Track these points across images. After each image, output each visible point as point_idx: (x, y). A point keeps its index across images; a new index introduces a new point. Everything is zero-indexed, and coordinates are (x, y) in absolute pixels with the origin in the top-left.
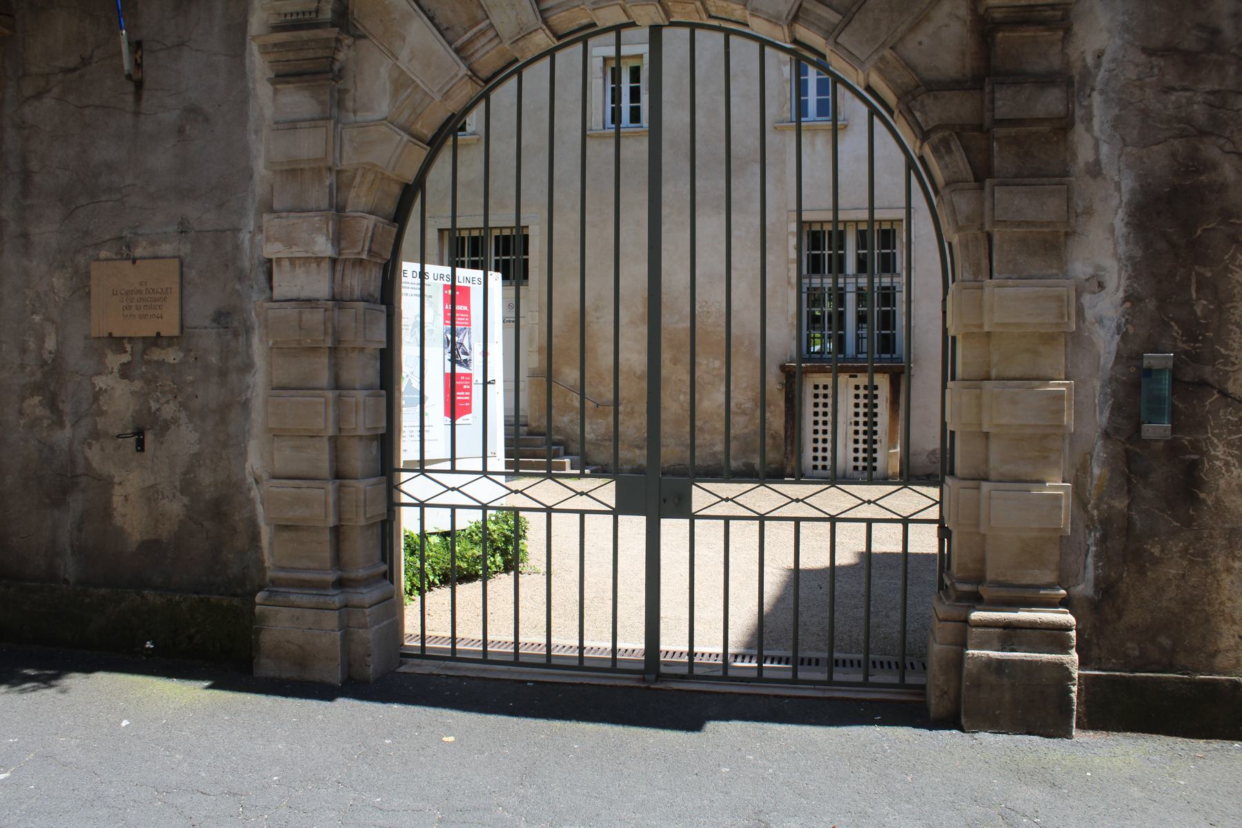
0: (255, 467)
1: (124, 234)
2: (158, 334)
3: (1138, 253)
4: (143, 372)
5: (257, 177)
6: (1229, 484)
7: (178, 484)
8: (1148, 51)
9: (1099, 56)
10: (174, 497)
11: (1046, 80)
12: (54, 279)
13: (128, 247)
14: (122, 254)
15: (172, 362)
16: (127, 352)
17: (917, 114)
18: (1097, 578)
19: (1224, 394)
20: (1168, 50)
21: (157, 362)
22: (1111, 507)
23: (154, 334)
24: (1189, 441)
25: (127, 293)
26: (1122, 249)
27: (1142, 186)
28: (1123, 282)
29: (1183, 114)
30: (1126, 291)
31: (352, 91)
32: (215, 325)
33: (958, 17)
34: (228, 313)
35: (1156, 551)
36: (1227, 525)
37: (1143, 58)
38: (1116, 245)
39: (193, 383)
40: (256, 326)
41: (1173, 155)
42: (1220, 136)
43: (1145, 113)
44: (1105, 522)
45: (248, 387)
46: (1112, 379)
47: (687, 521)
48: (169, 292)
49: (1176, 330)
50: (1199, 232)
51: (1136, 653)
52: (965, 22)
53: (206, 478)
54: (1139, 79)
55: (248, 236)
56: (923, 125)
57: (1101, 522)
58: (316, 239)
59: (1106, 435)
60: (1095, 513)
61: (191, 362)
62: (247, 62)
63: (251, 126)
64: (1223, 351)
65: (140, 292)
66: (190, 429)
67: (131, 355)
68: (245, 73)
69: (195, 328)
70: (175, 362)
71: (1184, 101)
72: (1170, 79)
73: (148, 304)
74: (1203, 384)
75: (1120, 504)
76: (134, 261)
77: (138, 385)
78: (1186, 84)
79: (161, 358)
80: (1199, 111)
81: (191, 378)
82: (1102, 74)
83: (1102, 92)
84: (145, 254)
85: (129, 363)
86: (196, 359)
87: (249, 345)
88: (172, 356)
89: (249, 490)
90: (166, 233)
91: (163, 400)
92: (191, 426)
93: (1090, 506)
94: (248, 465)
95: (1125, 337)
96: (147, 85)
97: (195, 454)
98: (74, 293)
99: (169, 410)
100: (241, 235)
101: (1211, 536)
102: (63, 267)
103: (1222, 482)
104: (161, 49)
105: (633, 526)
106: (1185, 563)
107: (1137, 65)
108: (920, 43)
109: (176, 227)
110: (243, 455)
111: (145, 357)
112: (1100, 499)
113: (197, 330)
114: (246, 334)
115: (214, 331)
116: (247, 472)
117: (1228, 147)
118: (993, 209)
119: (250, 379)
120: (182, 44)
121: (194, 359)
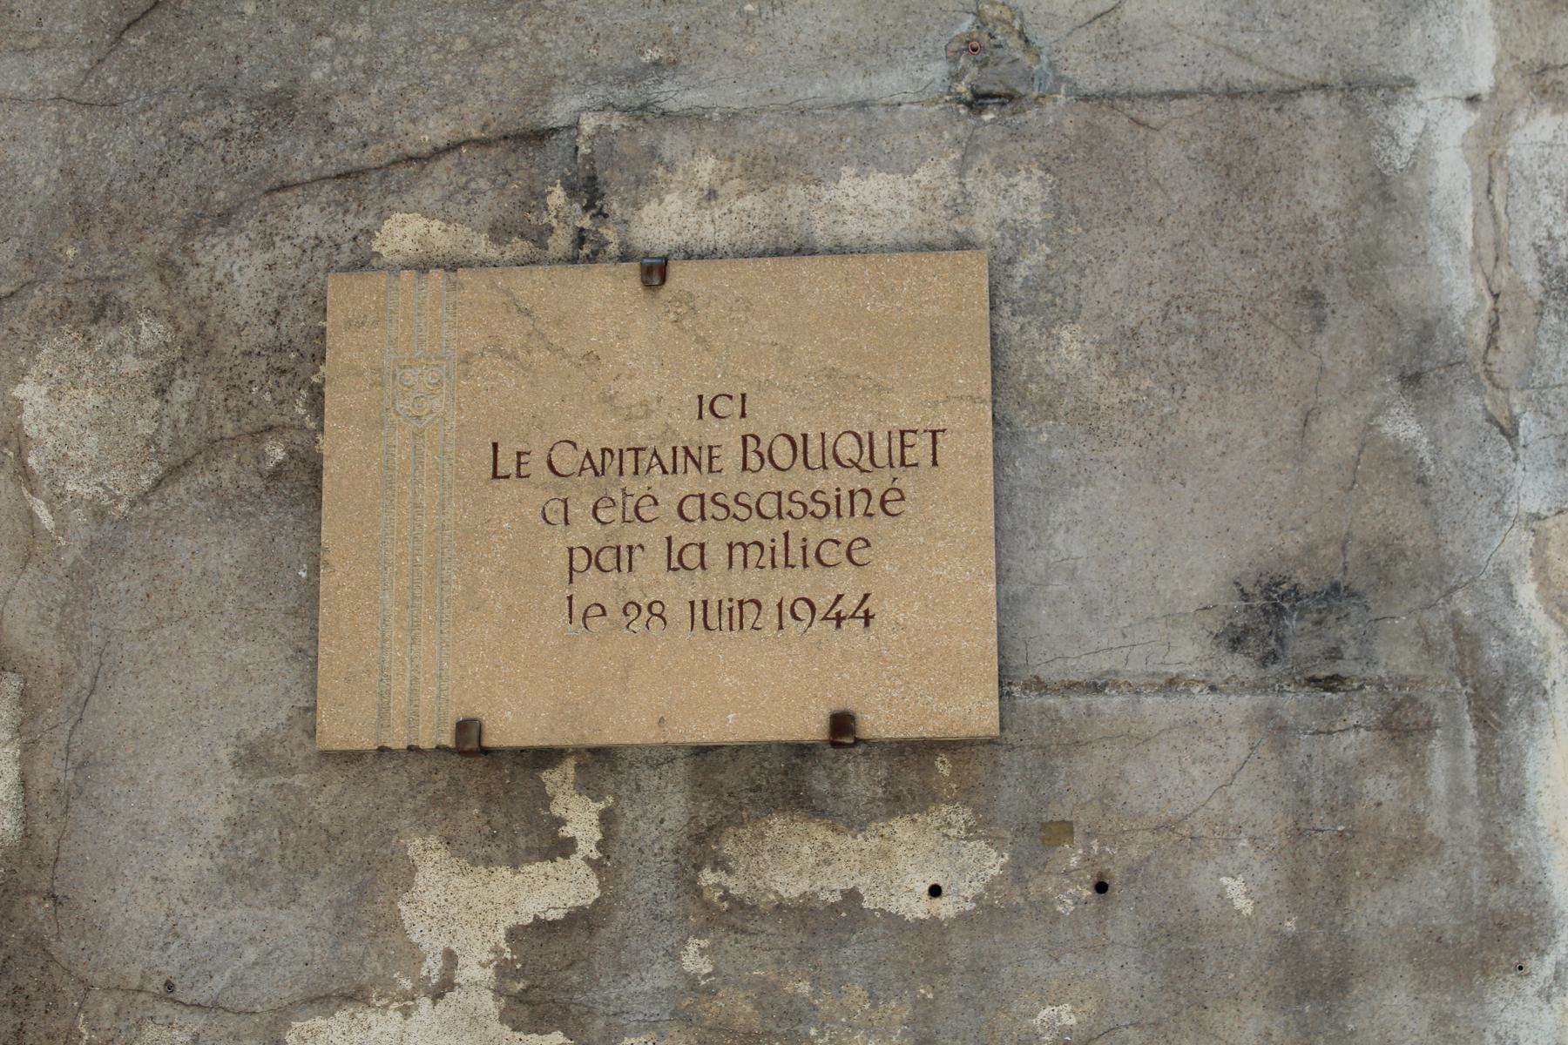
1: (559, 114)
2: (842, 724)
4: (692, 980)
12: (30, 392)
13: (589, 191)
14: (540, 236)
15: (917, 907)
16: (565, 848)
21: (803, 913)
23: (814, 728)
32: (1239, 666)
48: (920, 449)
61: (1066, 907)
65: (700, 458)
67: (596, 866)
69: (1096, 687)
70: (945, 908)
73: (758, 530)
76: (655, 272)
79: (831, 886)
84: (715, 229)
85: (581, 920)
86: (1101, 887)
90: (862, 105)
98: (175, 471)
100: (1410, 121)
102: (102, 310)
109: (937, 70)
111: (708, 877)
113: (1111, 704)
114: (1481, 722)
121: (1087, 893)
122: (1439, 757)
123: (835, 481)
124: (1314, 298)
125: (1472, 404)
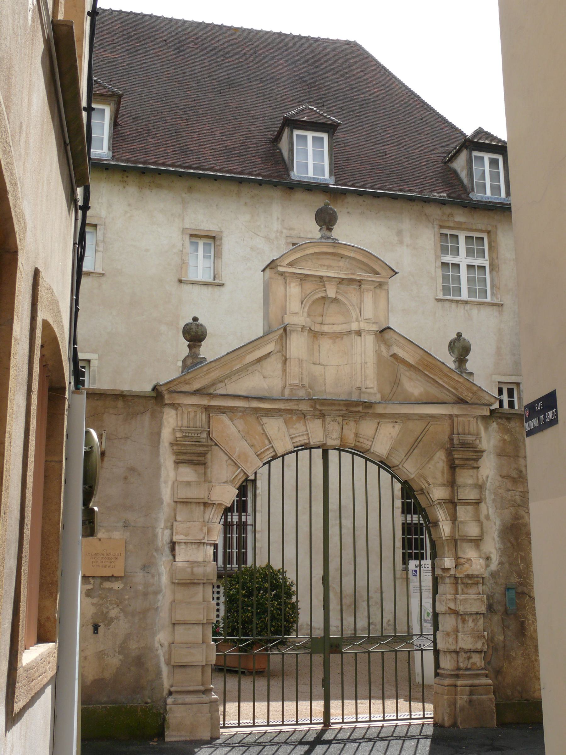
0: (160, 639)
3: (502, 547)
4: (100, 594)
5: (165, 503)
7: (117, 650)
8: (503, 477)
9: (487, 477)
10: (114, 656)
15: (117, 588)
16: (91, 584)
17: (431, 495)
20: (507, 477)
25: (95, 555)
26: (497, 546)
27: (502, 523)
28: (498, 558)
32: (142, 571)
33: (442, 459)
35: (514, 655)
37: (500, 479)
38: (495, 544)
39: (128, 599)
40: (164, 573)
43: (502, 498)
48: (119, 555)
51: (510, 694)
52: (444, 461)
53: (133, 645)
54: (500, 486)
55: (160, 531)
61: (128, 589)
63: (162, 479)
66: (125, 621)
70: (119, 589)
71: (513, 494)
72: (509, 486)
73: (107, 560)
74: (524, 593)
77: (95, 600)
79: (111, 587)
80: (518, 498)
81: (127, 597)
83: (489, 490)
85: (92, 589)
88: (117, 586)
89: (157, 650)
90: (116, 526)
91: (111, 608)
94: (157, 639)
96: (107, 454)
99: (114, 613)
103: (532, 628)
104: (115, 439)
105: (318, 659)
106: (523, 659)
108: (430, 468)
109: (122, 524)
111: (101, 586)
114: (159, 576)
115: (141, 574)
116: (156, 642)
119: (160, 597)
122: (155, 578)
123: (113, 557)
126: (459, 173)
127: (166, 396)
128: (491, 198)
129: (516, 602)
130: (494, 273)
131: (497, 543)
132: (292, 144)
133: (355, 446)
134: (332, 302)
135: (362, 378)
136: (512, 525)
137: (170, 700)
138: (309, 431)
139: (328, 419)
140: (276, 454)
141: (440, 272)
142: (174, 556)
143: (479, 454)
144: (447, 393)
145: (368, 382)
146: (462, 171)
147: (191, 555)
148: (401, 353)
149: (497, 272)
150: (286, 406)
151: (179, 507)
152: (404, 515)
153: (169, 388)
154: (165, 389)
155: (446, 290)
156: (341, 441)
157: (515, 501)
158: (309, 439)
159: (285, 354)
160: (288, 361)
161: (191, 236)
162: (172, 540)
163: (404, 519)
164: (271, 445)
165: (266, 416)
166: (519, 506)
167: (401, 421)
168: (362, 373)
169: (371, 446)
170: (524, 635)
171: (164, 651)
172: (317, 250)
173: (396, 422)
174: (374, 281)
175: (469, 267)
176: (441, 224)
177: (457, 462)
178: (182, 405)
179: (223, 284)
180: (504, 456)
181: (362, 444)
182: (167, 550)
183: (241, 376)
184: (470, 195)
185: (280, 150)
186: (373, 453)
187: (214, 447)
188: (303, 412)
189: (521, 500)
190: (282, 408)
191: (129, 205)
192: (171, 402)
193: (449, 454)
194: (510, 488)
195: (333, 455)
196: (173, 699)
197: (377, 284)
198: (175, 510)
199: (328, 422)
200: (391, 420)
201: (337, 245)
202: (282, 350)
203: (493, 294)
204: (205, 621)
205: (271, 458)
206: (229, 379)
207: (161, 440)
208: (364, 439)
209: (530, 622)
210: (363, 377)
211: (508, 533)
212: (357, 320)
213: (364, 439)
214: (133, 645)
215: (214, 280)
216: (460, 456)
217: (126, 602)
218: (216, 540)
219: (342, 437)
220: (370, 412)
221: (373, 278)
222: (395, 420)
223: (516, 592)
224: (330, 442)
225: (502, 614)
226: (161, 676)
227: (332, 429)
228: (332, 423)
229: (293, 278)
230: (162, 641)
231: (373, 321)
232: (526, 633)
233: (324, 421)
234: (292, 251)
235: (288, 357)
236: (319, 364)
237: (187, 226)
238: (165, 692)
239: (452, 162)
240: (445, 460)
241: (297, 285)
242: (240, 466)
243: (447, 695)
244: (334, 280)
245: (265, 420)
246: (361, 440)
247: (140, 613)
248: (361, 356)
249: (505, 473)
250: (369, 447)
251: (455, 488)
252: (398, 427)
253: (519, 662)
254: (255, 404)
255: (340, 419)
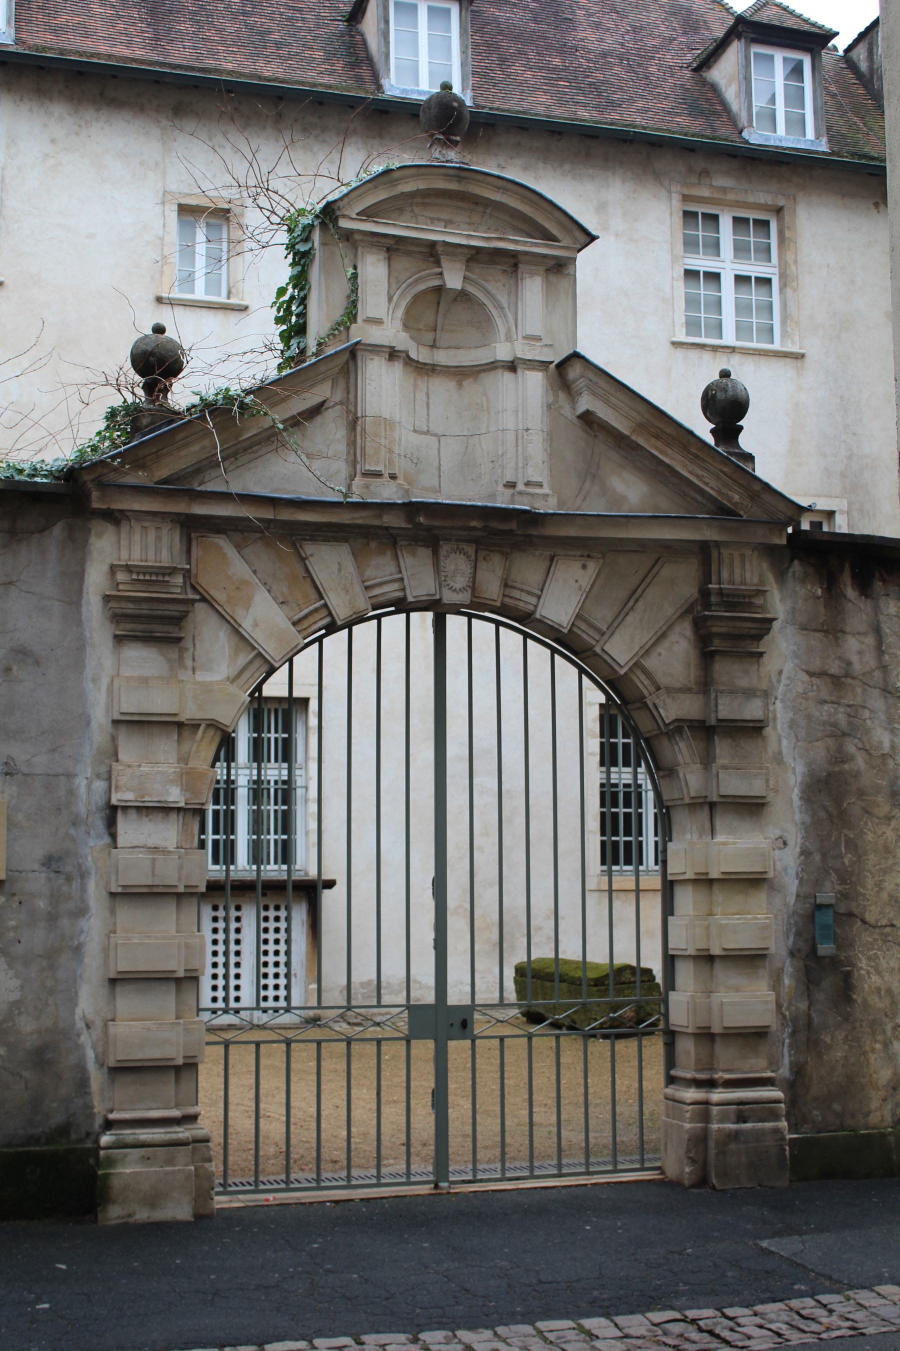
0: (86, 1012)
3: (808, 820)
5: (94, 725)
6: (870, 987)
8: (811, 674)
9: (780, 672)
11: (749, 693)
17: (661, 710)
18: (791, 1063)
19: (864, 922)
20: (822, 674)
22: (797, 1009)
24: (846, 957)
26: (797, 817)
28: (799, 841)
29: (832, 720)
30: (801, 848)
31: (191, 650)
32: (44, 869)
34: (60, 859)
35: (828, 1040)
36: (870, 1018)
37: (806, 678)
39: (15, 928)
40: (93, 872)
41: (827, 749)
42: (855, 737)
43: (809, 717)
44: (795, 1020)
45: (82, 932)
46: (794, 913)
47: (468, 1043)
49: (834, 876)
50: (845, 805)
51: (820, 1119)
53: (27, 1025)
54: (805, 693)
55: (84, 782)
56: (665, 719)
57: (792, 1021)
58: (170, 790)
59: (792, 954)
60: (787, 1013)
61: (14, 906)
62: (84, 610)
63: (89, 673)
64: (862, 890)
68: (81, 620)
71: (832, 710)
72: (824, 695)
74: (851, 915)
75: (803, 1006)
78: (833, 698)
80: (842, 718)
81: (13, 923)
82: (781, 689)
83: (782, 701)
86: (20, 903)
87: (83, 889)
89: (79, 1035)
92: (11, 973)
93: (783, 1009)
94: (78, 1011)
95: (801, 881)
97: (17, 1001)
100: (77, 781)
101: (861, 1026)
103: (866, 986)
105: (424, 1049)
106: (847, 1047)
107: (803, 683)
110: (73, 1002)
112: (790, 1003)
115: (44, 875)
116: (77, 1018)
117: (860, 745)
118: (718, 786)
119: (84, 923)
120: (10, 583)
122: (74, 884)
124: (59, 809)
125: (83, 828)
126: (723, 90)
127: (95, 494)
128: (786, 140)
129: (835, 932)
130: (789, 291)
131: (797, 810)
132: (387, 22)
133: (503, 605)
134: (455, 300)
135: (517, 464)
136: (829, 774)
137: (106, 1139)
138: (404, 572)
139: (444, 549)
140: (333, 622)
141: (680, 288)
142: (113, 836)
143: (766, 626)
144: (699, 498)
145: (530, 471)
146: (729, 85)
147: (150, 835)
148: (603, 412)
149: (795, 290)
150: (354, 519)
151: (123, 729)
152: (604, 769)
153: (100, 476)
154: (91, 477)
155: (692, 325)
156: (473, 595)
157: (834, 725)
158: (404, 589)
159: (353, 409)
160: (359, 423)
161: (183, 209)
162: (109, 800)
163: (604, 776)
164: (323, 602)
165: (313, 539)
166: (844, 734)
167: (600, 556)
168: (517, 451)
169: (536, 607)
170: (849, 1000)
171: (94, 1037)
172: (422, 185)
173: (589, 556)
174: (545, 256)
175: (741, 280)
176: (686, 192)
177: (717, 644)
178: (129, 514)
179: (246, 308)
180: (815, 630)
181: (517, 603)
182: (99, 824)
183: (260, 453)
184: (745, 134)
185: (362, 35)
186: (540, 621)
187: (200, 606)
188: (391, 531)
189: (850, 723)
190: (347, 522)
191: (53, 141)
192: (105, 507)
193: (699, 624)
194: (828, 698)
195: (455, 624)
196: (114, 1138)
197: (552, 262)
198: (114, 739)
199: (445, 553)
200: (579, 553)
201: (463, 174)
202: (348, 399)
203: (785, 334)
204: (181, 974)
205: (323, 631)
206: (233, 459)
207: (85, 589)
208: (522, 590)
209: (863, 972)
210: (520, 457)
211: (820, 791)
212: (509, 338)
213: (522, 590)
214: (27, 1025)
215: (229, 298)
216: (723, 630)
217: (12, 934)
218: (204, 801)
219: (473, 587)
220: (535, 533)
221: (541, 249)
222: (586, 554)
223: (836, 913)
224: (449, 597)
225: (807, 956)
226: (87, 1090)
227: (453, 568)
228: (453, 556)
229: (372, 245)
230: (90, 1017)
231: (545, 342)
232: (855, 997)
233: (435, 553)
234: (369, 185)
235: (359, 415)
236: (427, 432)
237: (173, 187)
238: (98, 1122)
239: (709, 68)
240: (692, 638)
241: (379, 260)
242: (256, 646)
243: (690, 1122)
244: (460, 250)
245: (309, 549)
246: (516, 594)
247: (40, 956)
248: (517, 415)
249: (816, 664)
250: (532, 608)
251: (713, 696)
252: (593, 567)
253: (839, 1054)
254: (287, 515)
255: (470, 549)
